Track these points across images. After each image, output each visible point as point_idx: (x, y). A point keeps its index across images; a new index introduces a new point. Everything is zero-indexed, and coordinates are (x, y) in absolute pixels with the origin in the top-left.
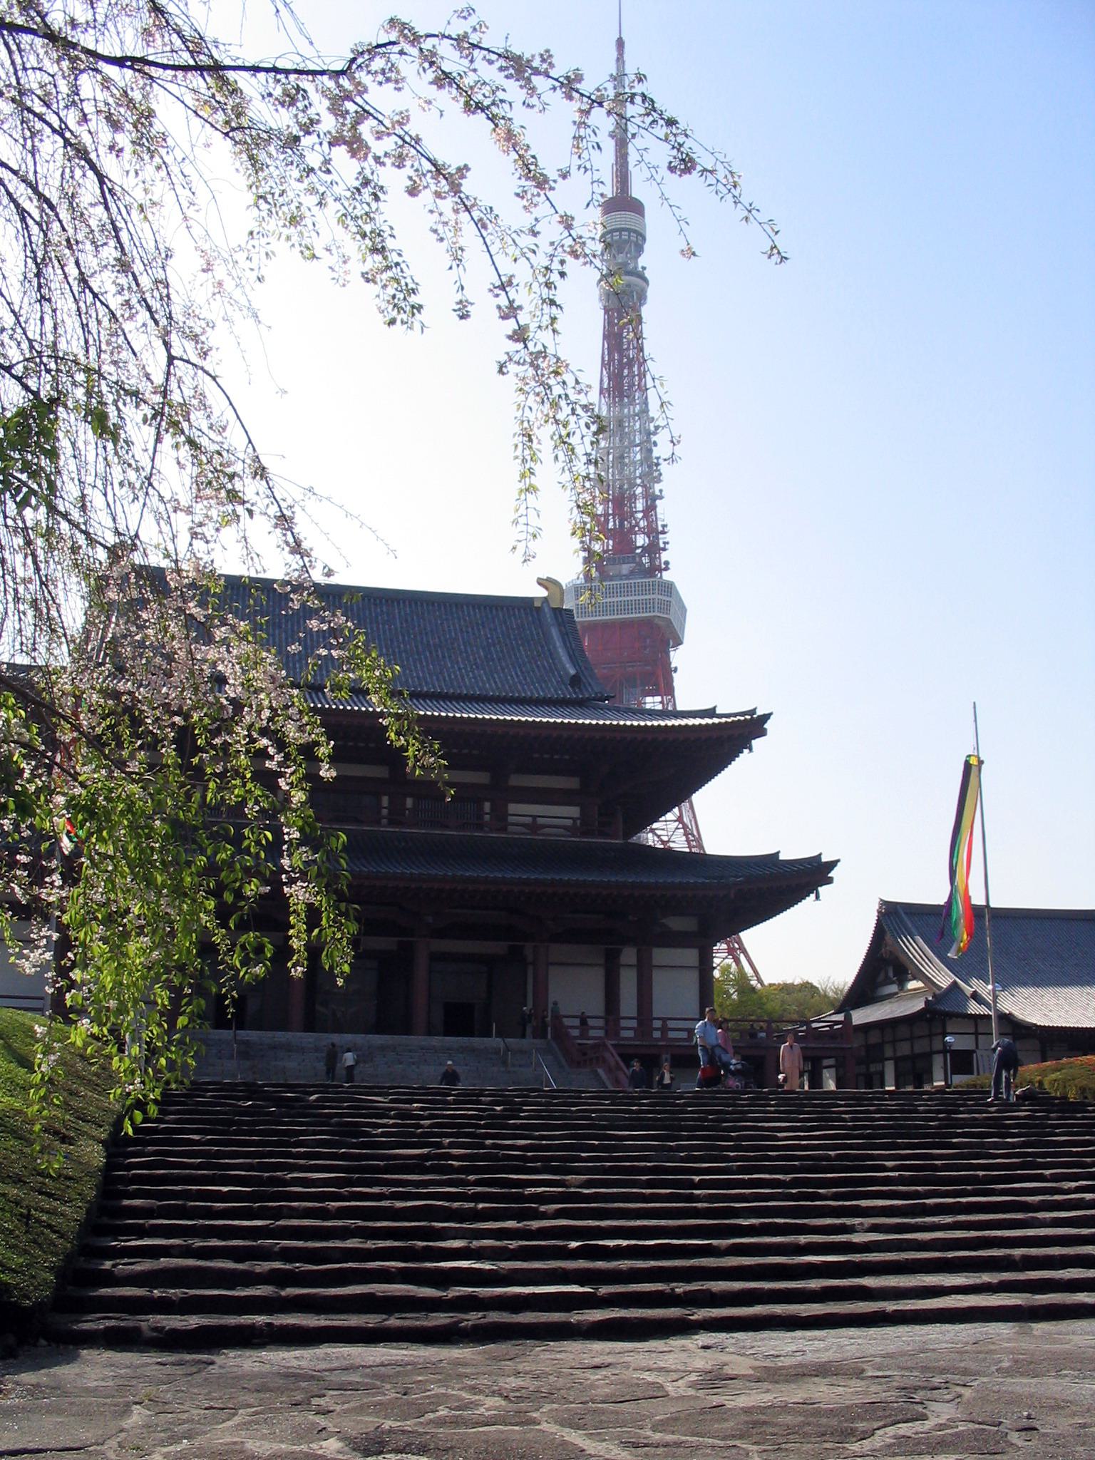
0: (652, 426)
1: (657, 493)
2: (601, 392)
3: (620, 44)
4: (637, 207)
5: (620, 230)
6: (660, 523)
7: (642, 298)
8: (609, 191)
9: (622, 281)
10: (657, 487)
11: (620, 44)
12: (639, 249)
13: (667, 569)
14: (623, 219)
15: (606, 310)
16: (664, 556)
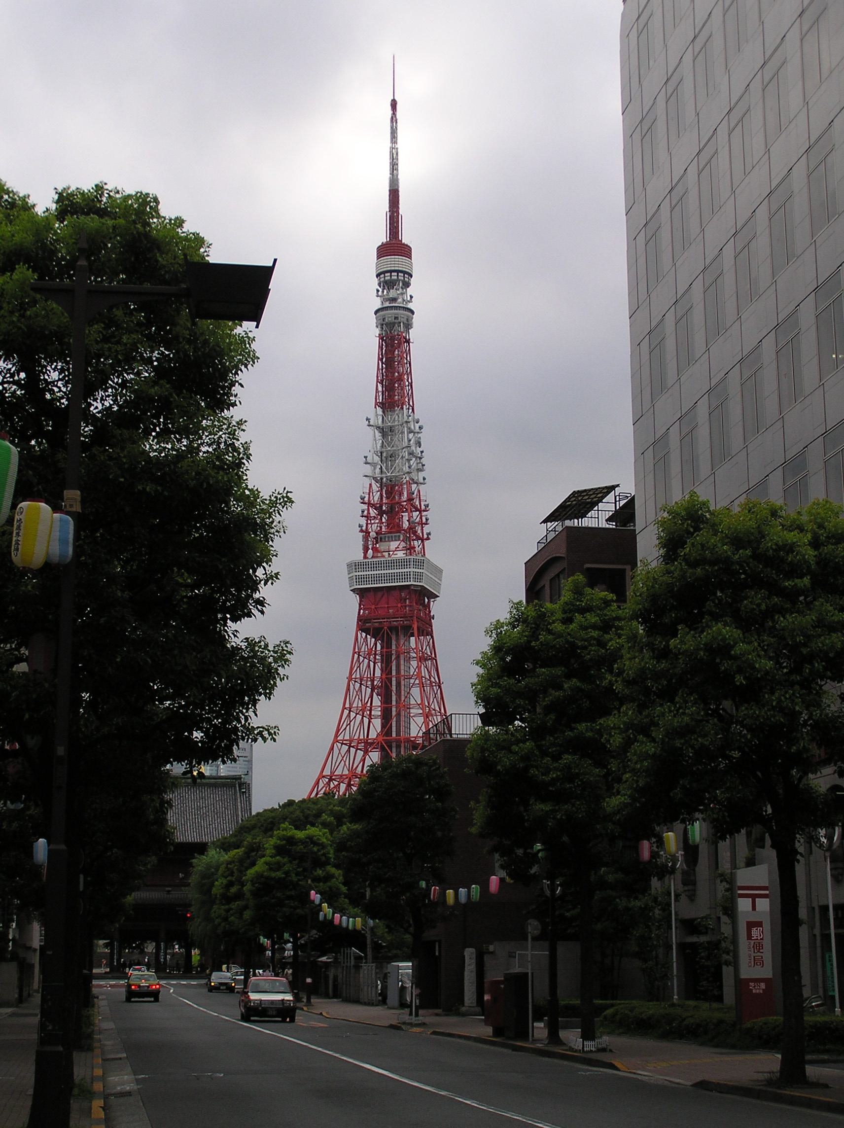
0: (417, 425)
1: (421, 480)
2: (376, 404)
3: (394, 104)
4: (405, 251)
5: (391, 272)
6: (422, 504)
7: (408, 326)
8: (382, 237)
9: (390, 315)
10: (421, 475)
11: (394, 104)
12: (407, 285)
13: (428, 539)
14: (395, 262)
15: (381, 337)
16: (426, 529)
